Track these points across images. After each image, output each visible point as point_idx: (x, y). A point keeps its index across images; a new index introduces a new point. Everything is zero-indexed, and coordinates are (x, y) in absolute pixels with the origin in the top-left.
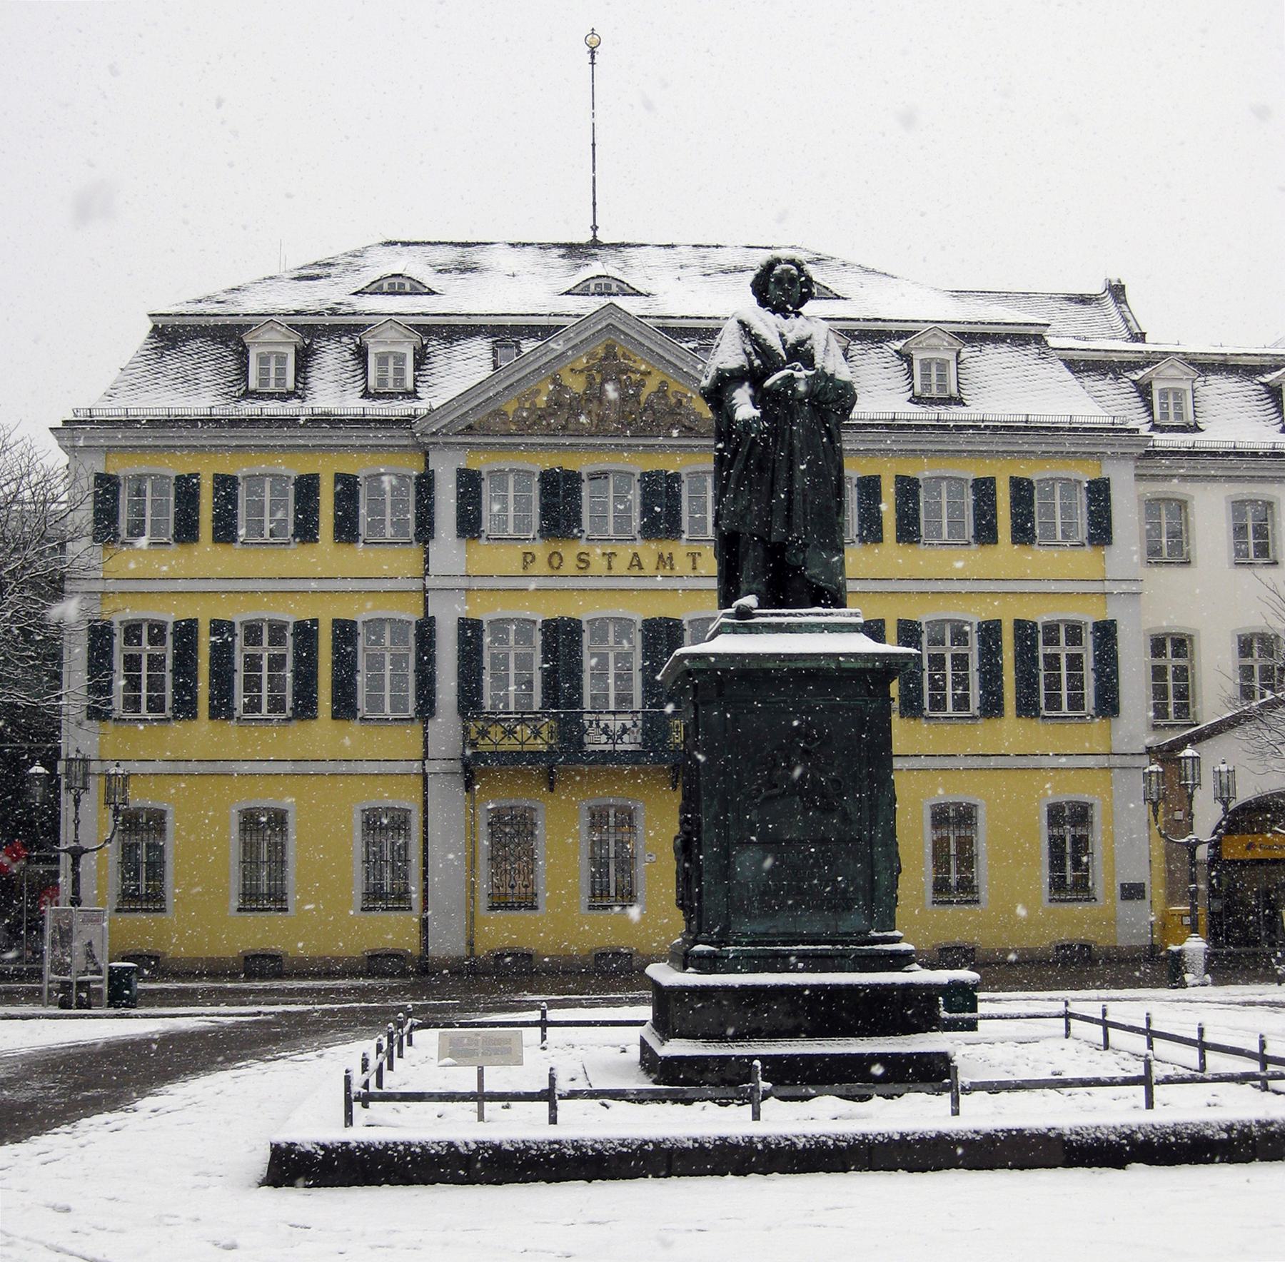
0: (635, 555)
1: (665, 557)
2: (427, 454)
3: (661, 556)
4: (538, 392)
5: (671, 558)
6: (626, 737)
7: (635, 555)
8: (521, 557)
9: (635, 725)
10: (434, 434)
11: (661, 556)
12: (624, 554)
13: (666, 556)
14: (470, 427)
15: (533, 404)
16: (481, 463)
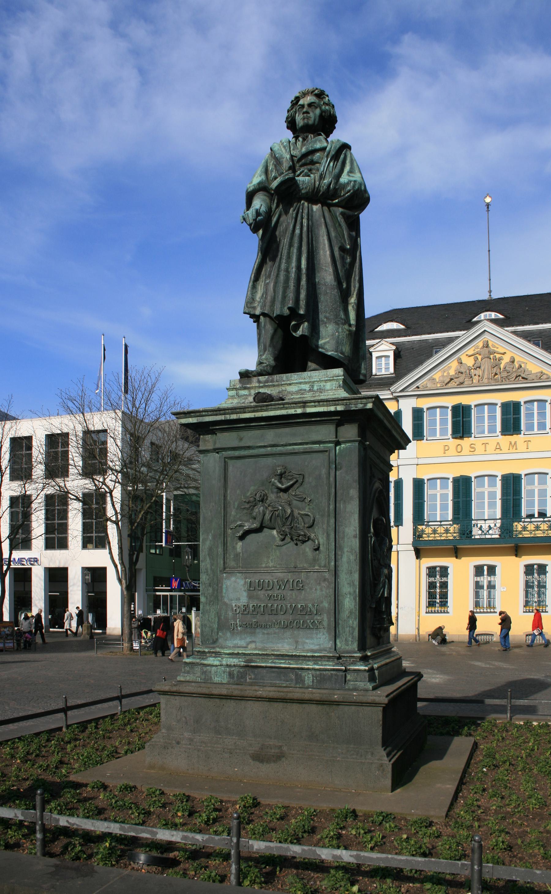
0: (498, 443)
1: (513, 443)
2: (398, 401)
3: (511, 443)
4: (450, 368)
5: (515, 443)
6: (491, 532)
7: (498, 443)
8: (443, 447)
9: (495, 525)
10: (402, 391)
11: (511, 443)
12: (492, 442)
13: (513, 443)
14: (418, 387)
15: (448, 373)
16: (424, 403)
